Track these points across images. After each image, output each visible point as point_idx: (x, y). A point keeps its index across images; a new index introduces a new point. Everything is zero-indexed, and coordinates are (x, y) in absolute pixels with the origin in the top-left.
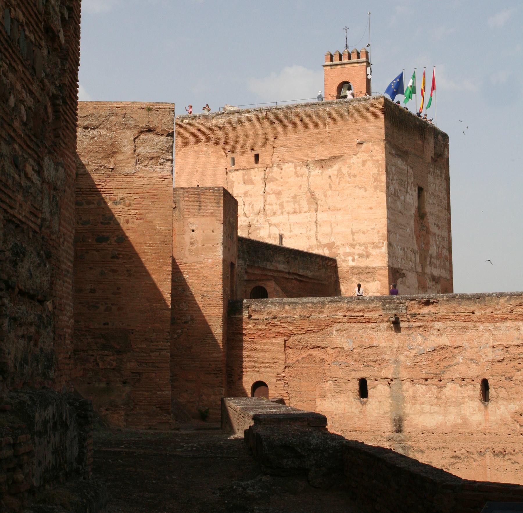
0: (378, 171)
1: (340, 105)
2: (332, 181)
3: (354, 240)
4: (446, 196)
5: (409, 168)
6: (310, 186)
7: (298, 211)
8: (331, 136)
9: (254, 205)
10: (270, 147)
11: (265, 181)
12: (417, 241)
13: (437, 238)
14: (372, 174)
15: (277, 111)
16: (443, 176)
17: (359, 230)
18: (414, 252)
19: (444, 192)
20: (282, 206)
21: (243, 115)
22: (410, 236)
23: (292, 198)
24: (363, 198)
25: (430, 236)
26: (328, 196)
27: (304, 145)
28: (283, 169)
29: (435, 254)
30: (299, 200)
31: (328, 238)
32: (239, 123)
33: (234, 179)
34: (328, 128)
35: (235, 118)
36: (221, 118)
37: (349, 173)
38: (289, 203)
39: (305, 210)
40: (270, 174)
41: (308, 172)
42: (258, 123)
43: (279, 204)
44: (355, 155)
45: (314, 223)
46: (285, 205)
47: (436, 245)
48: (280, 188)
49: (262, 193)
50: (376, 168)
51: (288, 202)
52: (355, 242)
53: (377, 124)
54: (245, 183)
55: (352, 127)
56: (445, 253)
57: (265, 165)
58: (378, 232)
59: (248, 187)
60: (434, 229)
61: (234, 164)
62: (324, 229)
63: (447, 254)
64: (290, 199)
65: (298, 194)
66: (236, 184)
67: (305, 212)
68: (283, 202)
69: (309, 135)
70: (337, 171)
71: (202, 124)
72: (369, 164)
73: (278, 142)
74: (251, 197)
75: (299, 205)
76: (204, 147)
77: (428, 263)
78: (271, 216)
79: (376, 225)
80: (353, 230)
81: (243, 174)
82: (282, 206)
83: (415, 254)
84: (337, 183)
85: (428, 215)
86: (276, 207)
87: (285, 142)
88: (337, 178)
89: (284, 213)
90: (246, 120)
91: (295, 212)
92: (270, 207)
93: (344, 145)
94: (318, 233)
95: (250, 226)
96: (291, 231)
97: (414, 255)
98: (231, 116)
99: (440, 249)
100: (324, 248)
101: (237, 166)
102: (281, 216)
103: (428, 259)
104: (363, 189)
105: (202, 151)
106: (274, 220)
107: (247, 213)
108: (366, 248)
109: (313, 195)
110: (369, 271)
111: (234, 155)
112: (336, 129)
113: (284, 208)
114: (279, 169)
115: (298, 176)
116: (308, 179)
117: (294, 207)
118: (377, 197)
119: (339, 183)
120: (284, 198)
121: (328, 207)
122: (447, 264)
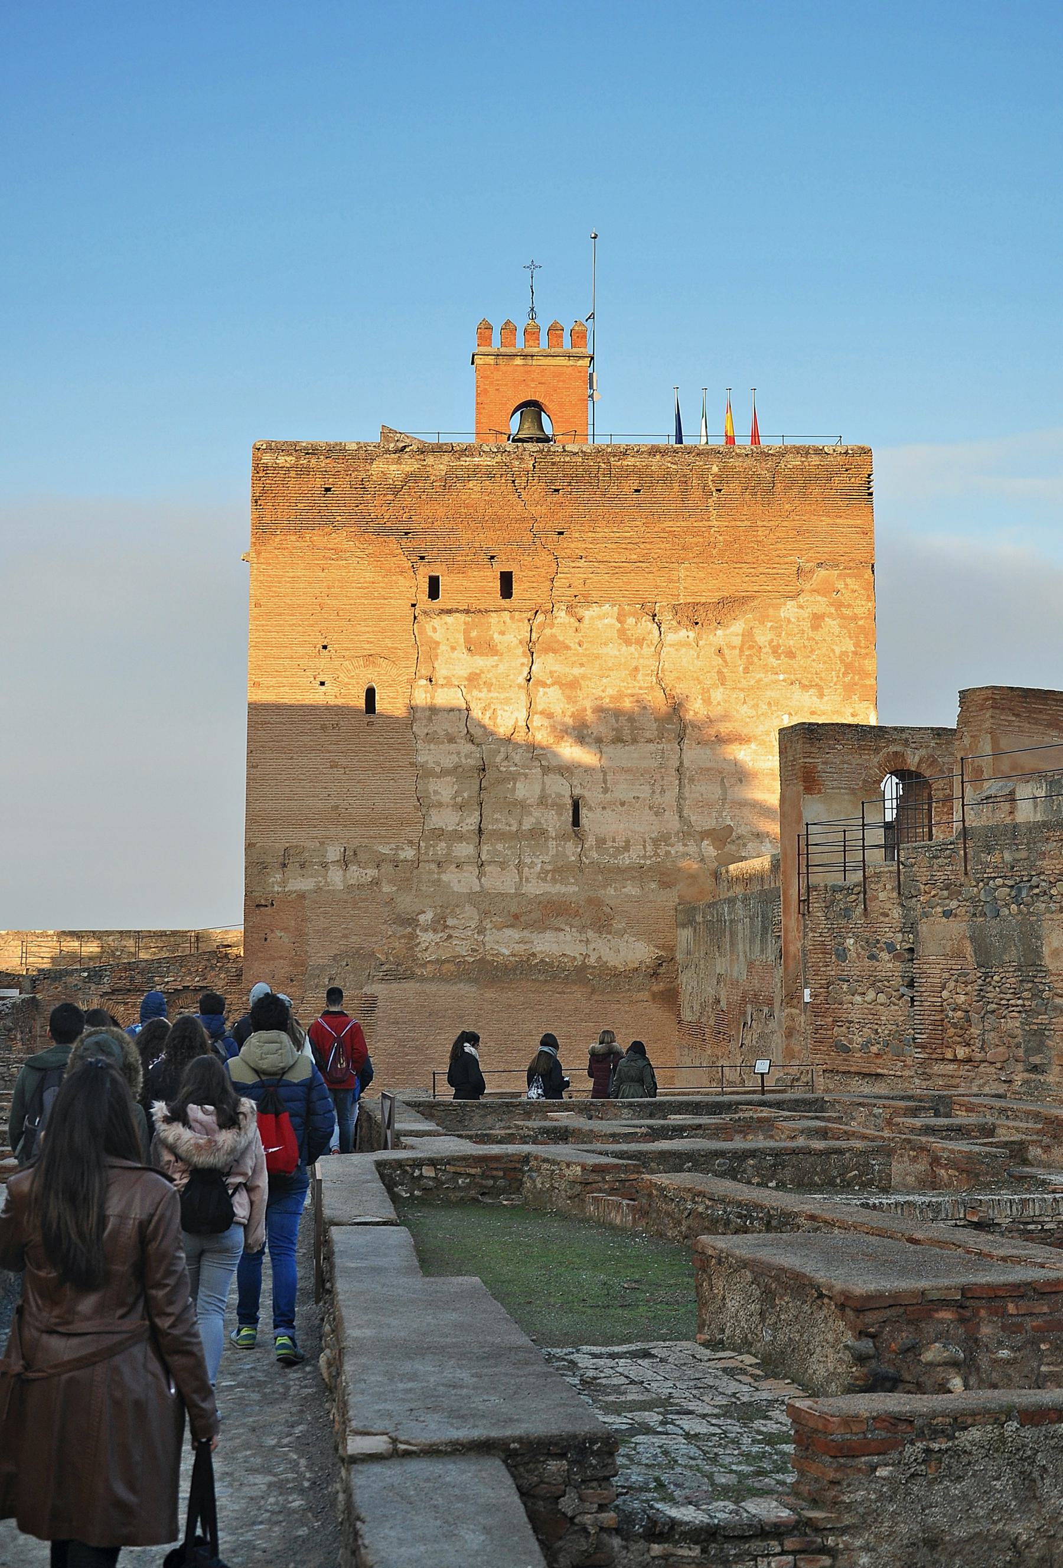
2: (725, 661)
8: (725, 540)
9: (499, 713)
14: (837, 653)
21: (466, 461)
26: (715, 703)
28: (586, 621)
31: (714, 814)
33: (437, 637)
35: (439, 466)
37: (774, 644)
40: (548, 631)
45: (674, 773)
48: (577, 671)
49: (521, 680)
50: (850, 637)
54: (470, 650)
55: (785, 524)
59: (480, 662)
66: (443, 648)
69: (662, 535)
70: (740, 638)
72: (832, 624)
73: (572, 545)
74: (489, 691)
76: (341, 539)
84: (741, 669)
87: (591, 546)
88: (740, 656)
89: (587, 739)
90: (474, 472)
91: (618, 740)
93: (761, 570)
94: (685, 799)
95: (484, 770)
96: (606, 790)
98: (430, 460)
100: (702, 840)
104: (812, 691)
112: (739, 523)
115: (628, 642)
118: (853, 715)
119: (746, 671)
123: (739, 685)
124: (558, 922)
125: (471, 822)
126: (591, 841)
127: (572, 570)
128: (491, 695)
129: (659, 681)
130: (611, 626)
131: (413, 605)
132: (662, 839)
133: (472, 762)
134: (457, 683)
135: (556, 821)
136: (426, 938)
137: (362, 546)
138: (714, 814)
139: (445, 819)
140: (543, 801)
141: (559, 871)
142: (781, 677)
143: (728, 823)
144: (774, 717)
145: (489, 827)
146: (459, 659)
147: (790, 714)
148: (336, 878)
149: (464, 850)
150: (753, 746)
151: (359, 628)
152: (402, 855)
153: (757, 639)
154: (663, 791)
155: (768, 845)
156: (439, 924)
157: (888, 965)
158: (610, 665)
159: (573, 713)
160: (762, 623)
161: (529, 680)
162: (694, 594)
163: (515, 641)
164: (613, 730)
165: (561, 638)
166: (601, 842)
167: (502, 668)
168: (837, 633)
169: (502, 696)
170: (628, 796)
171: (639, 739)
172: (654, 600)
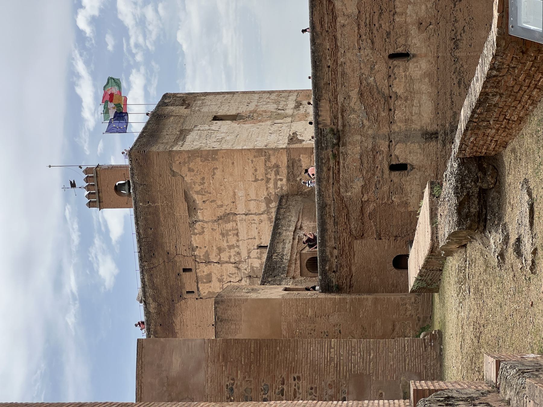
0: (198, 157)
1: (137, 192)
2: (207, 200)
3: (262, 180)
4: (222, 96)
5: (195, 129)
6: (212, 220)
7: (236, 232)
8: (166, 201)
9: (230, 272)
10: (177, 258)
11: (208, 262)
12: (263, 122)
13: (259, 104)
14: (202, 163)
15: (143, 251)
16: (203, 98)
17: (253, 174)
18: (273, 124)
19: (218, 97)
20: (231, 247)
21: (147, 283)
22: (258, 128)
23: (224, 237)
24: (223, 171)
25: (259, 110)
26: (222, 203)
27: (174, 226)
28: (197, 245)
29: (275, 106)
30: (226, 230)
32: (154, 287)
33: (207, 292)
35: (149, 291)
36: (150, 304)
37: (200, 184)
38: (229, 240)
39: (235, 225)
40: (202, 257)
41: (199, 223)
42: (154, 269)
43: (230, 249)
45: (247, 217)
46: (230, 244)
47: (266, 104)
48: (215, 248)
49: (219, 266)
50: (196, 159)
51: (227, 242)
52: (264, 178)
53: (155, 158)
55: (158, 181)
56: (273, 96)
57: (193, 263)
58: (255, 157)
59: (214, 279)
60: (252, 107)
61: (193, 292)
62: (252, 206)
63: (275, 94)
64: (225, 239)
65: (220, 231)
66: (210, 290)
67: (237, 224)
68: (228, 245)
69: (165, 221)
70: (199, 195)
72: (191, 165)
73: (172, 250)
74: (224, 275)
75: (230, 230)
76: (177, 321)
77: (283, 112)
78: (241, 257)
79: (248, 159)
80: (253, 180)
81: (201, 283)
82: (231, 247)
83: (275, 123)
84: (209, 195)
85: (238, 112)
87: (172, 244)
88: (205, 195)
89: (238, 244)
90: (151, 280)
91: (237, 235)
92: (233, 257)
93: (175, 189)
94: (256, 213)
95: (250, 276)
96: (255, 238)
97: (275, 124)
98: (148, 294)
99: (271, 101)
100: (270, 207)
101: (194, 289)
102: (241, 247)
103: (280, 112)
104: (215, 171)
106: (244, 255)
107: (238, 279)
108: (270, 168)
109: (220, 218)
110: (291, 165)
111: (184, 291)
112: (159, 196)
113: (233, 244)
114: (197, 250)
115: (203, 232)
116: (206, 222)
117: (232, 235)
118: (223, 158)
119: (210, 193)
121: (232, 204)
122: (283, 95)
123: (215, 195)
127: (180, 250)
128: (225, 275)
130: (198, 237)
131: (197, 299)
132: (270, 219)
133: (248, 280)
134: (222, 286)
137: (179, 315)
138: (260, 203)
140: (258, 258)
142: (211, 182)
143: (263, 199)
144: (225, 184)
146: (214, 285)
147: (224, 179)
150: (236, 191)
151: (206, 315)
153: (198, 190)
154: (254, 220)
155: (270, 185)
158: (212, 237)
159: (229, 249)
160: (193, 188)
161: (219, 263)
162: (185, 211)
163: (206, 267)
164: (234, 236)
165: (204, 253)
168: (194, 163)
169: (225, 271)
170: (256, 231)
171: (236, 228)
172: (188, 224)
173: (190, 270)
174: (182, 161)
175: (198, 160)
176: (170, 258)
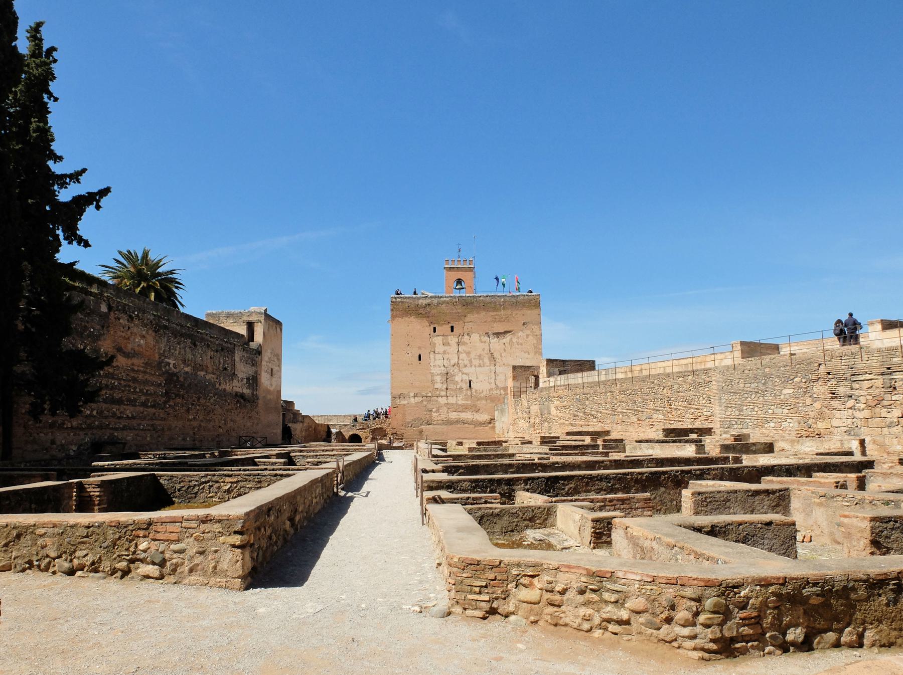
10: (461, 322)
20: (470, 361)
21: (442, 299)
27: (486, 321)
32: (438, 304)
34: (502, 312)
35: (435, 301)
44: (522, 331)
48: (470, 350)
51: (475, 359)
59: (446, 348)
64: (477, 357)
66: (437, 345)
71: (411, 303)
72: (531, 337)
73: (467, 319)
76: (412, 319)
82: (470, 361)
86: (466, 362)
91: (480, 366)
96: (477, 378)
98: (433, 299)
105: (411, 321)
106: (465, 370)
107: (446, 365)
111: (435, 326)
115: (482, 342)
120: (472, 355)
124: (466, 410)
125: (445, 386)
126: (474, 391)
129: (490, 351)
132: (491, 389)
135: (465, 386)
136: (434, 415)
139: (438, 386)
140: (462, 380)
141: (466, 398)
145: (449, 388)
148: (412, 400)
149: (443, 393)
152: (428, 395)
156: (437, 411)
157: (525, 415)
166: (476, 391)
167: (451, 349)
173: (452, 331)
174: (534, 330)
175: (535, 342)
176: (461, 317)
